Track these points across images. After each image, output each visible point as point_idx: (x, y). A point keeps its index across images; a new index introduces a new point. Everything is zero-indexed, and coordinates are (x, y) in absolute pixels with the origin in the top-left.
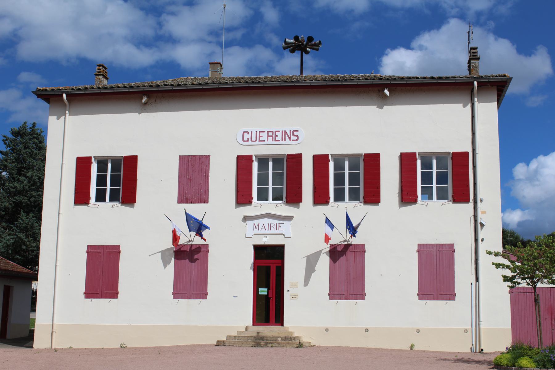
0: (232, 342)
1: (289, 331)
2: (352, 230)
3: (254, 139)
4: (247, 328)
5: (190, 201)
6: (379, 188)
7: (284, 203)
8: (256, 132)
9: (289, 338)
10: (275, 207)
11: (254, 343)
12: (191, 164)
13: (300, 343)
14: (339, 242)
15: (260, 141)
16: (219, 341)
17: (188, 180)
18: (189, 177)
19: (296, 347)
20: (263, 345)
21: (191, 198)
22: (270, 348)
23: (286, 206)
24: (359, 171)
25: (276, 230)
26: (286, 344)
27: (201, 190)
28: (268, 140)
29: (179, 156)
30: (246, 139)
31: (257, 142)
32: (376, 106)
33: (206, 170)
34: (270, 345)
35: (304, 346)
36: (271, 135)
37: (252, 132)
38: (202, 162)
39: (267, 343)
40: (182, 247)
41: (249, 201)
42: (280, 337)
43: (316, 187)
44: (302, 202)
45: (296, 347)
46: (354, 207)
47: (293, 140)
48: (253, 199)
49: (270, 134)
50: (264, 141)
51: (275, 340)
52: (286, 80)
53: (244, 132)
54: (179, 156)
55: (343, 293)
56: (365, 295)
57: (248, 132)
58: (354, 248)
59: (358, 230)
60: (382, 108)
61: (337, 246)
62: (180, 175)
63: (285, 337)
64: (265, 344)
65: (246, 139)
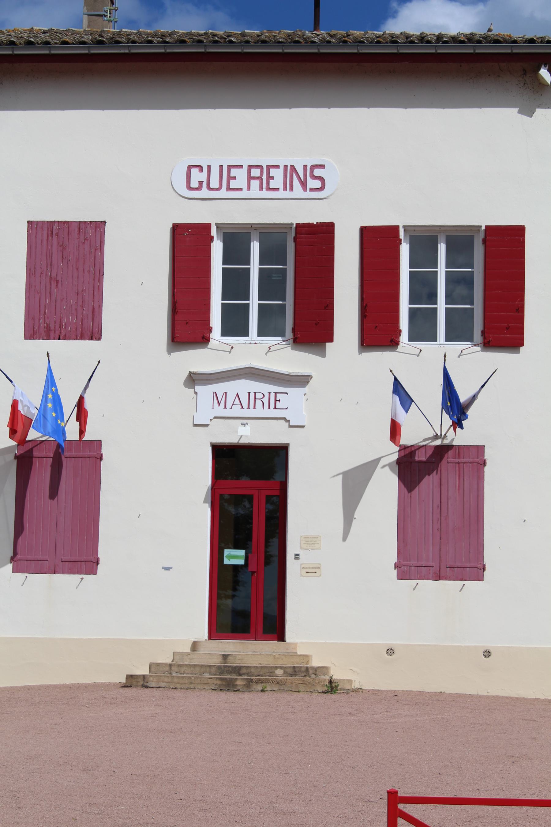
0: (166, 680)
1: (299, 653)
2: (456, 412)
3: (214, 183)
4: (195, 646)
6: (520, 310)
7: (287, 342)
8: (221, 167)
9: (303, 669)
10: (266, 354)
11: (219, 682)
12: (59, 243)
13: (331, 682)
14: (422, 440)
15: (229, 189)
16: (132, 676)
17: (51, 283)
18: (54, 275)
19: (323, 692)
20: (241, 685)
23: (292, 349)
24: (472, 267)
25: (269, 408)
27: (82, 306)
28: (249, 188)
29: (28, 222)
30: (194, 184)
31: (224, 193)
32: (517, 110)
33: (95, 258)
34: (259, 687)
35: (341, 689)
36: (258, 175)
37: (209, 167)
38: (86, 239)
39: (251, 680)
40: (37, 445)
41: (203, 338)
42: (281, 668)
43: (366, 305)
44: (332, 341)
45: (323, 692)
46: (459, 357)
47: (312, 190)
49: (256, 172)
50: (241, 189)
51: (268, 674)
52: (296, 39)
53: (190, 167)
54: (28, 222)
55: (430, 563)
56: (484, 569)
57: (200, 168)
58: (459, 455)
59: (470, 412)
60: (530, 114)
61: (415, 450)
62: (30, 269)
63: (294, 667)
65: (194, 184)
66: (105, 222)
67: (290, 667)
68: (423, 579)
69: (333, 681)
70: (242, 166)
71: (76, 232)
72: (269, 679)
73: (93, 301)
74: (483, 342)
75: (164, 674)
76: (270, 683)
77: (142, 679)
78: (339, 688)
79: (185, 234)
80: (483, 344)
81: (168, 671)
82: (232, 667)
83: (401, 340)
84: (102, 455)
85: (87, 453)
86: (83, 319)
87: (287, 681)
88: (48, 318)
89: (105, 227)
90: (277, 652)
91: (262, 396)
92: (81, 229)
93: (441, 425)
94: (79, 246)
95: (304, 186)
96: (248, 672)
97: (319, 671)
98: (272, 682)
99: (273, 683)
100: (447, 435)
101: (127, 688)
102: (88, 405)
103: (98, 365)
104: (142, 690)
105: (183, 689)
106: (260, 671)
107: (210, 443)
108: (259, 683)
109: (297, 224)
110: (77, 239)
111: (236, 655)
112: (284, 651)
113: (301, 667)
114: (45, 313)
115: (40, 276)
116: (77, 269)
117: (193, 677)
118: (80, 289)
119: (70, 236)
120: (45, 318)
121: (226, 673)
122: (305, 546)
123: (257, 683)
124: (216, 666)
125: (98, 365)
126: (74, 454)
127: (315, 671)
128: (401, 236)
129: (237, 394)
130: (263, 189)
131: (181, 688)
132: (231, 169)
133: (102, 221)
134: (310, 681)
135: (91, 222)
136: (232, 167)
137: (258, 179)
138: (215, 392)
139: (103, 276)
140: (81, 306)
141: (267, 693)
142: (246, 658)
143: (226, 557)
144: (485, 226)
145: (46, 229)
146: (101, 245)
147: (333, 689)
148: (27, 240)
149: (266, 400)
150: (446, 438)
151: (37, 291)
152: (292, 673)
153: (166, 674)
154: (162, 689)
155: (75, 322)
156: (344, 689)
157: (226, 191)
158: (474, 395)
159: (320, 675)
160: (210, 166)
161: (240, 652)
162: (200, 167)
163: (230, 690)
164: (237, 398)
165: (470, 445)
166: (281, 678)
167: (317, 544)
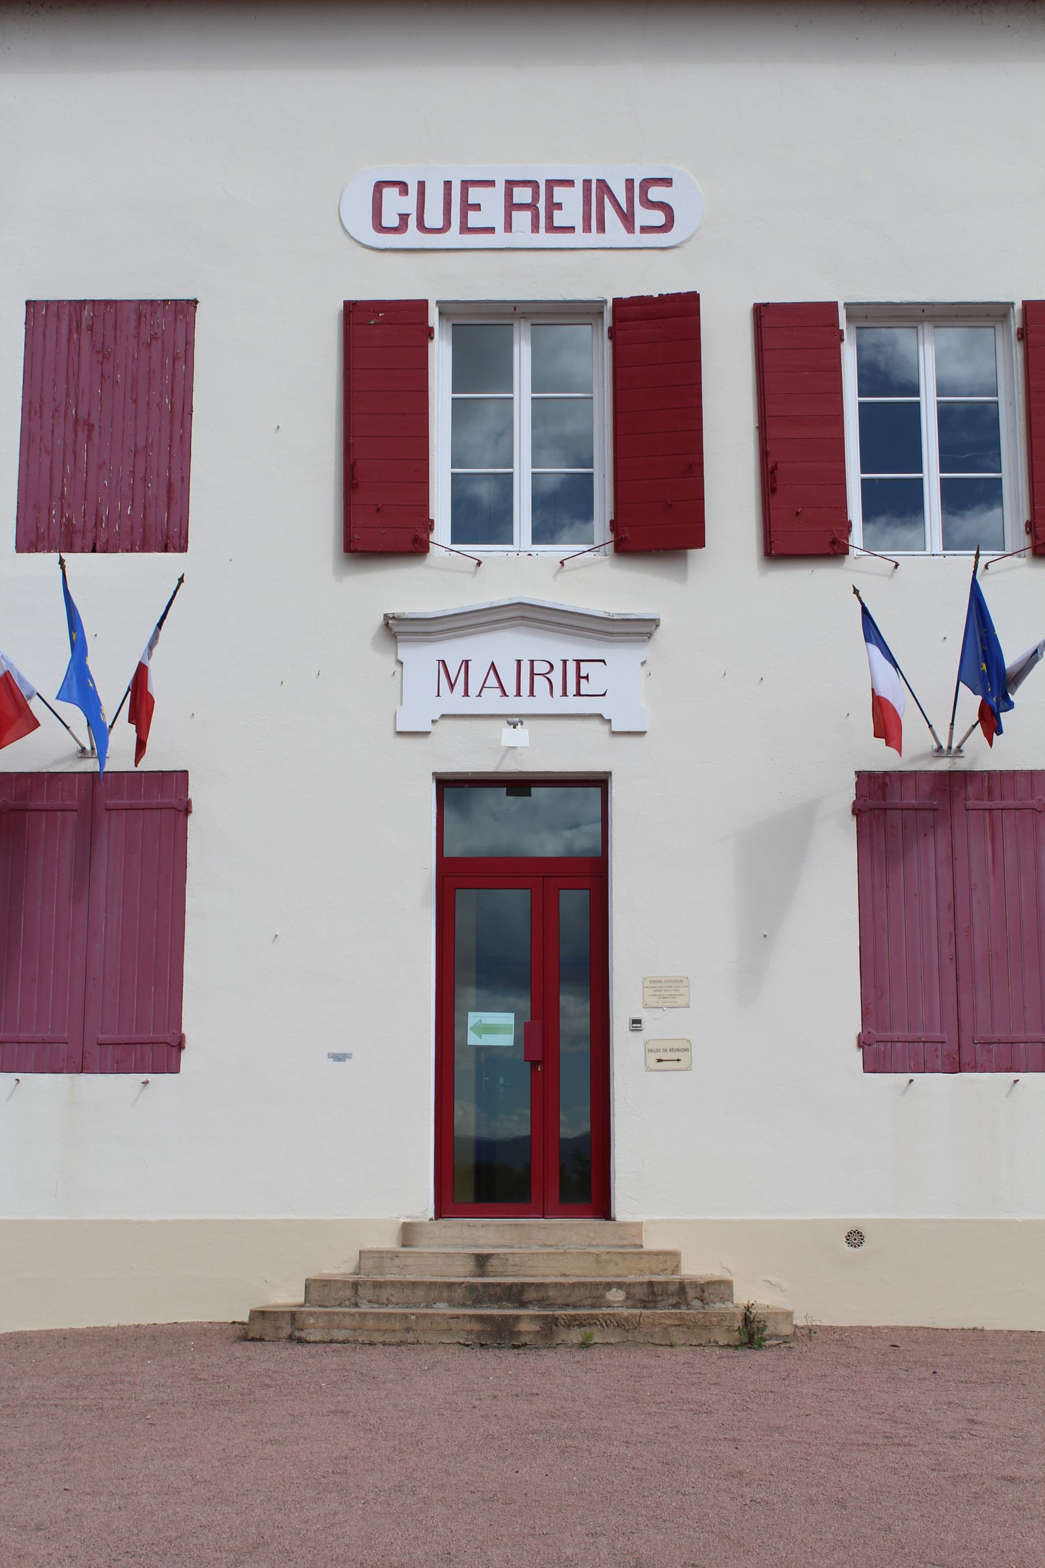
0: (348, 1322)
3: (434, 217)
4: (408, 1232)
5: (84, 537)
8: (448, 184)
9: (672, 1288)
11: (476, 1326)
13: (747, 1319)
15: (465, 229)
18: (83, 414)
19: (728, 1345)
20: (530, 1332)
21: (90, 525)
22: (580, 1355)
25: (565, 694)
26: (666, 1329)
28: (508, 227)
29: (28, 303)
30: (390, 219)
31: (453, 238)
33: (173, 375)
34: (575, 1336)
35: (771, 1337)
36: (528, 200)
37: (422, 185)
39: (555, 1320)
42: (620, 1286)
43: (775, 468)
45: (728, 1345)
47: (645, 229)
48: (431, 529)
49: (522, 195)
50: (491, 230)
51: (589, 1301)
53: (380, 186)
54: (28, 303)
55: (937, 1034)
57: (403, 187)
58: (990, 792)
62: (31, 402)
63: (651, 1284)
64: (543, 1329)
65: (390, 219)
66: (196, 302)
67: (641, 1284)
68: (923, 1070)
69: (754, 1318)
70: (494, 181)
71: (133, 323)
72: (597, 1315)
73: (170, 468)
74: (1030, 546)
75: (340, 1305)
76: (601, 1325)
77: (290, 1322)
78: (766, 1333)
79: (372, 322)
80: (1029, 552)
81: (349, 1299)
82: (503, 1285)
83: (850, 543)
84: (189, 803)
85: (157, 800)
86: (147, 507)
87: (642, 1320)
88: (69, 506)
89: (195, 311)
90: (597, 1246)
91: (547, 668)
92: (143, 316)
93: (952, 724)
94: (138, 352)
95: (629, 222)
96: (540, 1298)
97: (710, 1291)
98: (606, 1322)
99: (607, 1325)
100: (962, 748)
101: (251, 1342)
102: (155, 686)
103: (178, 587)
104: (290, 1351)
105: (389, 1345)
106: (570, 1295)
107: (433, 773)
108: (574, 1327)
109: (614, 299)
110: (135, 337)
111: (507, 1256)
112: (614, 1243)
113: (667, 1283)
114: (63, 494)
115: (53, 416)
116: (135, 401)
117: (413, 1314)
118: (141, 444)
119: (119, 331)
120: (62, 506)
121: (489, 1301)
122: (652, 1001)
123: (569, 1326)
124: (465, 1285)
125: (178, 587)
126: (125, 802)
127: (701, 1292)
128: (842, 324)
129: (493, 664)
130: (540, 230)
131: (384, 1341)
132: (470, 189)
133: (188, 300)
134: (697, 1318)
135: (165, 302)
136: (470, 184)
137: (527, 209)
138: (443, 661)
139: (191, 415)
140: (141, 479)
141: (594, 1352)
142: (531, 1263)
143: (471, 1028)
144: (1023, 302)
145: (66, 317)
146: (186, 349)
147: (754, 1338)
148: (25, 342)
149: (556, 677)
150: (961, 755)
151: (46, 448)
152: (646, 1299)
153: (346, 1306)
154: (339, 1345)
155: (129, 513)
156: (777, 1336)
157: (460, 234)
158: (1033, 650)
159: (712, 1302)
160: (424, 182)
161: (512, 1247)
162: (402, 186)
163: (503, 1345)
164: (492, 673)
165: (1014, 771)
166: (626, 1312)
167: (680, 995)
